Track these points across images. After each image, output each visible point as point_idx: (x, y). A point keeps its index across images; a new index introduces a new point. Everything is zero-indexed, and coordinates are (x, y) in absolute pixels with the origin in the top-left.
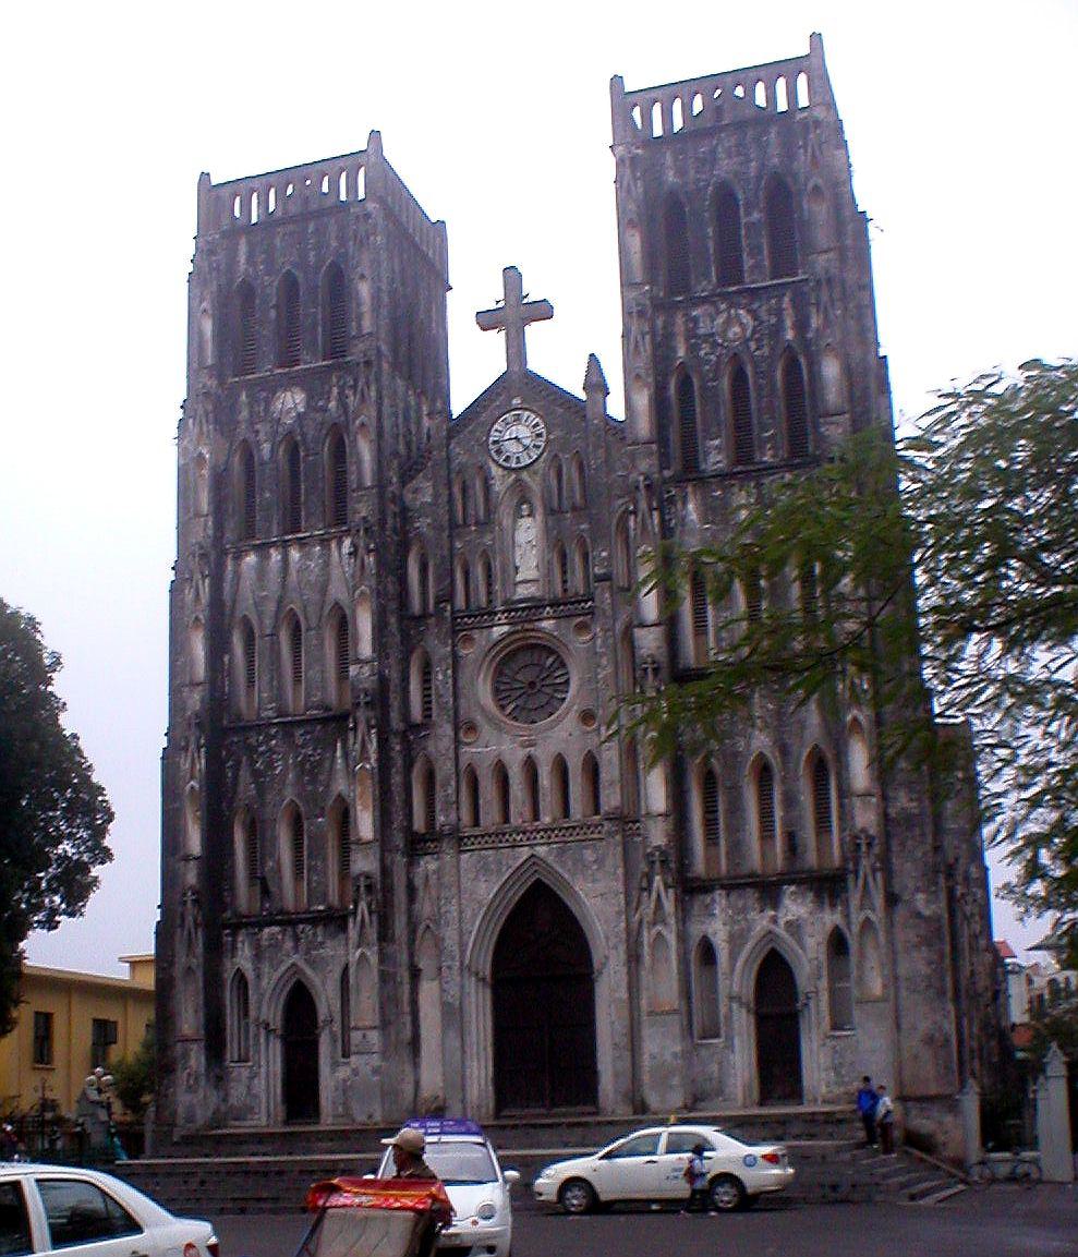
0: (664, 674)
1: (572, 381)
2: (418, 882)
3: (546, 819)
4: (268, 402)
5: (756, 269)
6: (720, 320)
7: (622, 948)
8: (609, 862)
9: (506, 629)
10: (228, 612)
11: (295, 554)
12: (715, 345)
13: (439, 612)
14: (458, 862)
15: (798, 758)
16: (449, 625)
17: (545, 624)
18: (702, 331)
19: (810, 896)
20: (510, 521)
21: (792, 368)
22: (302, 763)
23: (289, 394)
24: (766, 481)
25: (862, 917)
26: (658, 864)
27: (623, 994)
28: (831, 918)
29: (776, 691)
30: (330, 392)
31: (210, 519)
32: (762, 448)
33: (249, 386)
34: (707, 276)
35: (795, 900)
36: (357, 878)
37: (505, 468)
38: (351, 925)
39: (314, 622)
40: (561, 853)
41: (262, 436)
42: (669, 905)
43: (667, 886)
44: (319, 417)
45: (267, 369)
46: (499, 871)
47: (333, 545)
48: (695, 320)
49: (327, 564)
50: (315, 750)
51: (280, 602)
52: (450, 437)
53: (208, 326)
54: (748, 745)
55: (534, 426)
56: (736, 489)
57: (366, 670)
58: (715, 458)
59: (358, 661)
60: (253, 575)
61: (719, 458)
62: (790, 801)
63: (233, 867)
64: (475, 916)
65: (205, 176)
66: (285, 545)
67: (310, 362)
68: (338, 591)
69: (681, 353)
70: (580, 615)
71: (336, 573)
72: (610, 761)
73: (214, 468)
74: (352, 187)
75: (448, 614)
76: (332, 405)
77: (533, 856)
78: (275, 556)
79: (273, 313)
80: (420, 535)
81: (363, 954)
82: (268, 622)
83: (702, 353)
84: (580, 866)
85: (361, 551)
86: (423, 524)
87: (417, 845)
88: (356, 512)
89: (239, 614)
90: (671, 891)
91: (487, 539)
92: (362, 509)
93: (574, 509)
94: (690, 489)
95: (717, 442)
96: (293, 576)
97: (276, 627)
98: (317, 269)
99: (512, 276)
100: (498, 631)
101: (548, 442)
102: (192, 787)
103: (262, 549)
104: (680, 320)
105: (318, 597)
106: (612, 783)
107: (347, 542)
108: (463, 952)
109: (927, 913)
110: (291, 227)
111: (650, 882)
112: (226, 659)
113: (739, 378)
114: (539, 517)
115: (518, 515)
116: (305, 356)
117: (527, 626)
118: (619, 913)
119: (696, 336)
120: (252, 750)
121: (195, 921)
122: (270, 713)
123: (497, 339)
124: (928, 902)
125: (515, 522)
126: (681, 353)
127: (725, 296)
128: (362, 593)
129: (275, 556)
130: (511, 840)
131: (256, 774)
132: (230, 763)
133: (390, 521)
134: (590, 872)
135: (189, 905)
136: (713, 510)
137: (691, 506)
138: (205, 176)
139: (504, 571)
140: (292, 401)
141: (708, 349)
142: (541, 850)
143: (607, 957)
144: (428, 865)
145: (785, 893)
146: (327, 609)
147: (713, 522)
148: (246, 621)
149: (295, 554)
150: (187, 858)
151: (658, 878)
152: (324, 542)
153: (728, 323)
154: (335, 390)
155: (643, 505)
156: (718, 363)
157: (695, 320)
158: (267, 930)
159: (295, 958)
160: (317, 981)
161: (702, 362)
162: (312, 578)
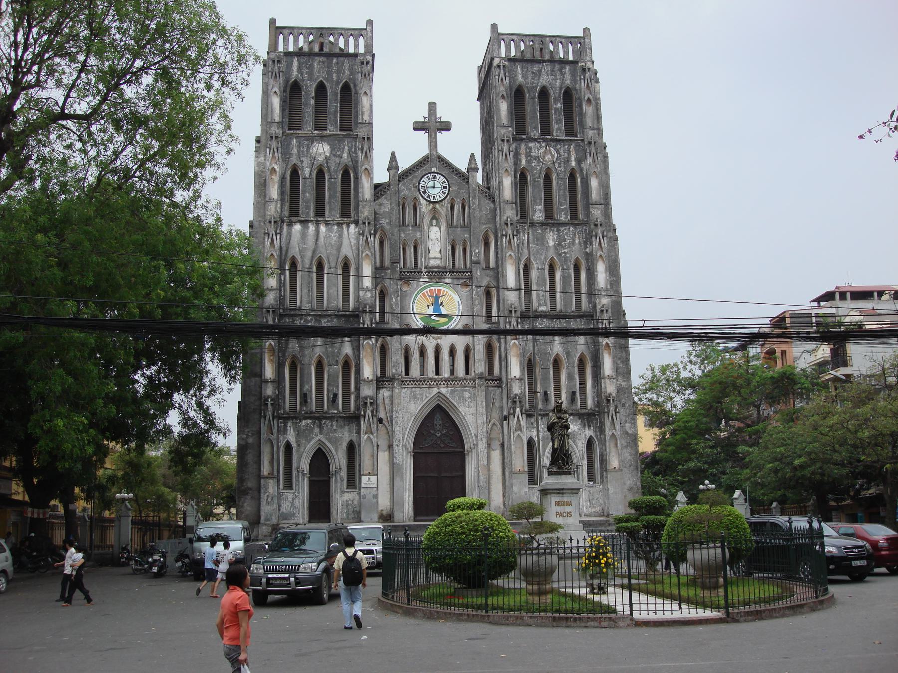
0: (518, 314)
1: (463, 166)
2: (380, 401)
4: (309, 147)
5: (558, 128)
6: (542, 150)
7: (485, 440)
8: (479, 399)
10: (284, 253)
11: (323, 228)
12: (539, 161)
13: (393, 269)
18: (533, 154)
21: (572, 177)
24: (562, 229)
25: (610, 433)
27: (486, 463)
28: (589, 432)
30: (344, 148)
31: (279, 203)
32: (560, 214)
33: (298, 136)
34: (536, 128)
36: (366, 398)
38: (362, 423)
39: (333, 265)
40: (453, 393)
42: (523, 422)
44: (337, 160)
45: (308, 128)
46: (422, 400)
47: (345, 227)
48: (531, 148)
49: (341, 236)
51: (314, 252)
52: (399, 181)
53: (276, 102)
54: (552, 350)
56: (548, 231)
57: (369, 294)
58: (539, 215)
59: (363, 289)
60: (298, 235)
63: (285, 386)
64: (408, 420)
65: (273, 22)
66: (317, 223)
67: (332, 129)
68: (347, 250)
69: (524, 162)
71: (345, 242)
74: (356, 46)
76: (345, 155)
78: (312, 228)
79: (312, 101)
81: (368, 437)
84: (463, 399)
85: (366, 233)
86: (384, 222)
88: (362, 213)
89: (290, 255)
90: (524, 416)
91: (418, 235)
92: (365, 212)
96: (322, 240)
97: (311, 264)
98: (338, 82)
99: (432, 106)
101: (449, 191)
103: (304, 223)
104: (523, 146)
105: (335, 252)
106: (480, 361)
107: (352, 226)
109: (630, 432)
110: (323, 59)
111: (514, 411)
112: (283, 277)
113: (548, 178)
114: (443, 228)
115: (431, 225)
116: (330, 127)
118: (483, 423)
119: (530, 156)
121: (273, 415)
123: (423, 136)
124: (630, 428)
126: (524, 162)
127: (545, 140)
129: (312, 228)
135: (270, 406)
136: (538, 240)
138: (273, 22)
140: (322, 149)
142: (443, 391)
143: (476, 445)
144: (385, 393)
146: (340, 260)
148: (294, 258)
149: (323, 228)
150: (266, 382)
151: (518, 410)
152: (340, 225)
153: (545, 152)
154: (346, 148)
155: (510, 232)
156: (541, 170)
157: (531, 148)
158: (304, 421)
159: (320, 437)
160: (333, 449)
161: (533, 168)
162: (333, 242)
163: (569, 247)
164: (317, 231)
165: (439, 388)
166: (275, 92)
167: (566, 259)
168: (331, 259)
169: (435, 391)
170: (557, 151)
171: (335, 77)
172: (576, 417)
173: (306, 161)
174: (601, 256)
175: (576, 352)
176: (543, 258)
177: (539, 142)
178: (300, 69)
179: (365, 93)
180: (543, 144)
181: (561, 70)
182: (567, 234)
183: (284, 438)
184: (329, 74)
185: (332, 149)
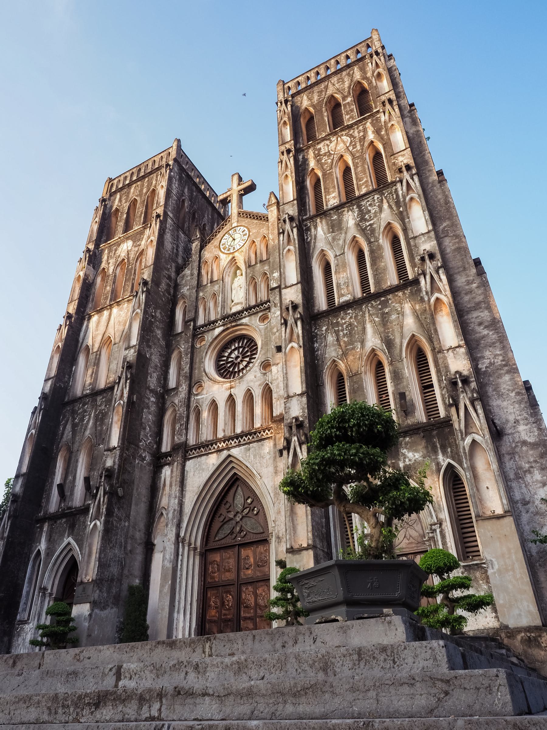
0: (300, 309)
3: (238, 431)
9: (221, 328)
10: (79, 345)
14: (183, 466)
15: (401, 346)
16: (191, 333)
17: (244, 321)
19: (423, 443)
20: (230, 279)
22: (98, 415)
23: (126, 244)
26: (294, 429)
29: (380, 309)
35: (409, 450)
37: (227, 254)
41: (110, 265)
43: (300, 445)
44: (136, 249)
48: (320, 149)
50: (106, 406)
55: (243, 232)
56: (345, 213)
61: (335, 201)
62: (397, 376)
70: (261, 311)
72: (278, 387)
73: (85, 280)
75: (191, 327)
77: (229, 456)
79: (125, 216)
80: (183, 297)
81: (95, 524)
82: (97, 346)
83: (323, 161)
86: (185, 290)
87: (159, 461)
89: (84, 345)
90: (304, 447)
93: (261, 261)
94: (318, 220)
95: (333, 195)
100: (217, 331)
102: (32, 433)
108: (179, 526)
109: (531, 440)
117: (233, 324)
120: (74, 413)
122: (88, 391)
125: (233, 280)
127: (335, 134)
128: (137, 313)
130: (216, 447)
131: (74, 426)
132: (64, 422)
133: (163, 286)
134: (265, 461)
137: (319, 229)
139: (224, 301)
141: (326, 158)
142: (235, 452)
144: (166, 472)
145: (401, 444)
147: (333, 232)
151: (295, 439)
159: (71, 539)
162: (121, 320)
163: (375, 216)
164: (110, 315)
165: (228, 449)
166: (96, 222)
167: (373, 231)
168: (117, 334)
169: (225, 453)
170: (351, 136)
171: (145, 191)
172: (416, 438)
173: (112, 261)
174: (412, 199)
175: (402, 337)
176: (341, 242)
177: (329, 139)
178: (120, 200)
179: (162, 186)
180: (334, 139)
181: (348, 74)
182: (370, 205)
183: (37, 547)
184: (141, 191)
185: (134, 242)
